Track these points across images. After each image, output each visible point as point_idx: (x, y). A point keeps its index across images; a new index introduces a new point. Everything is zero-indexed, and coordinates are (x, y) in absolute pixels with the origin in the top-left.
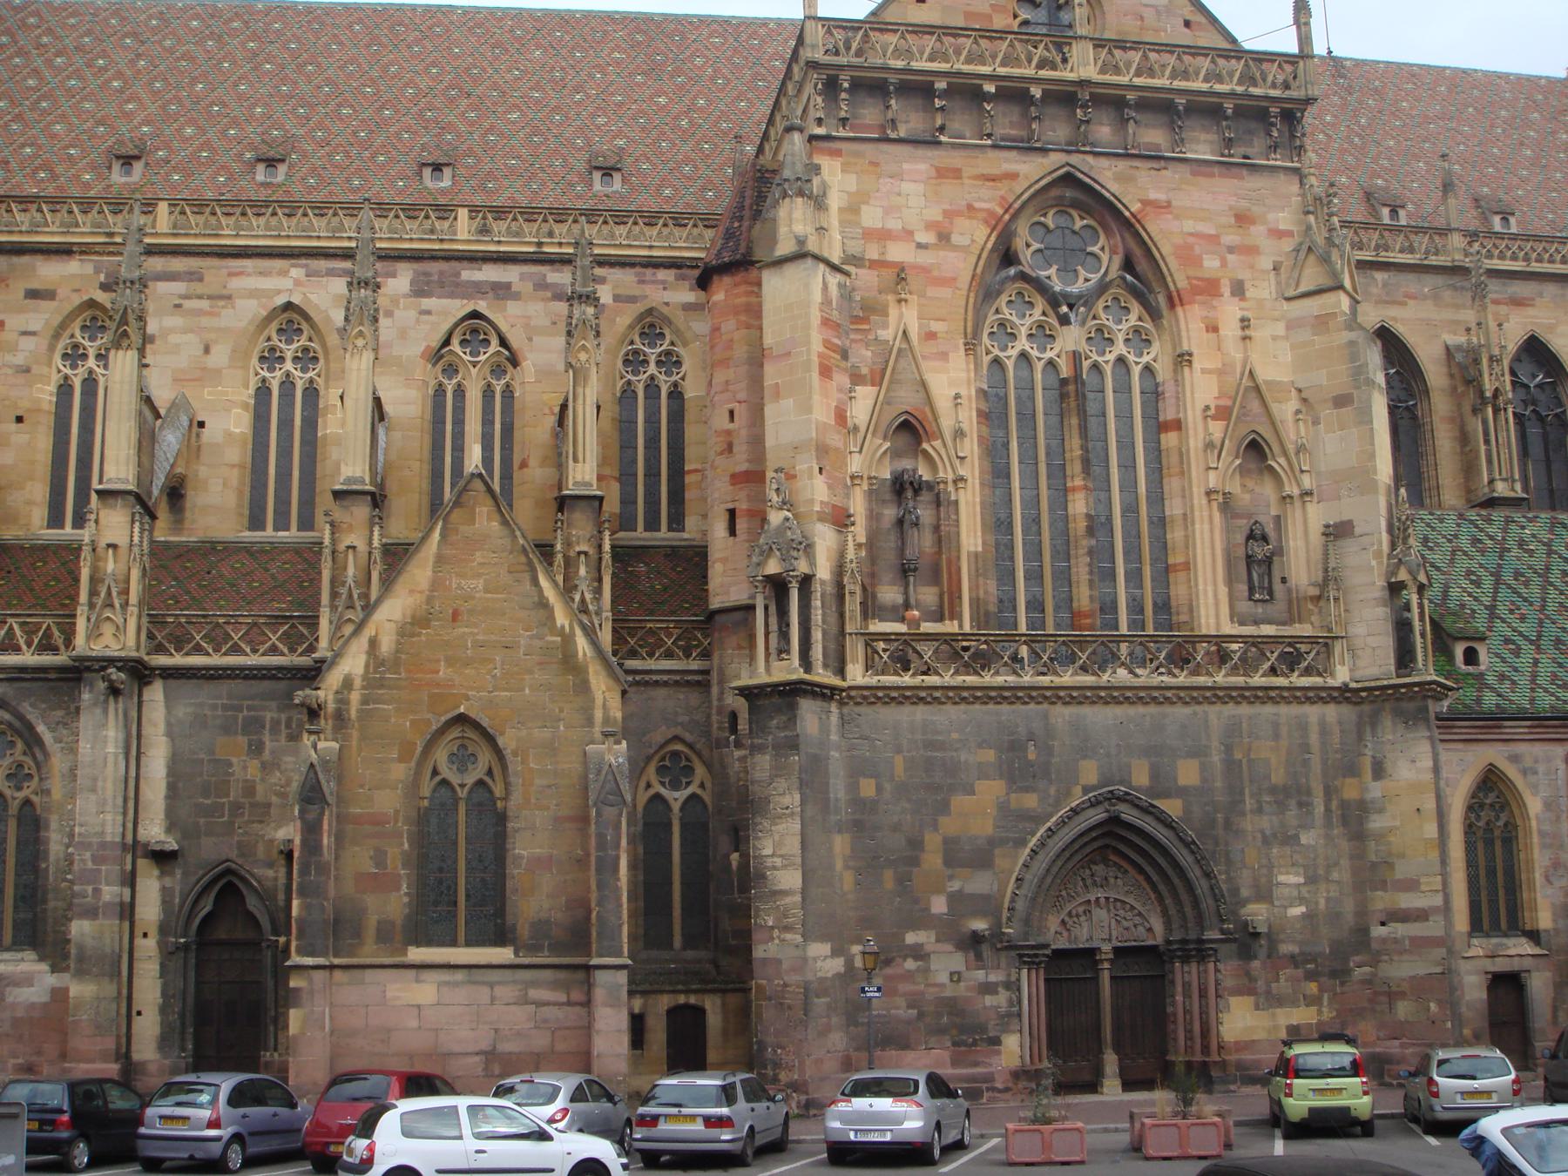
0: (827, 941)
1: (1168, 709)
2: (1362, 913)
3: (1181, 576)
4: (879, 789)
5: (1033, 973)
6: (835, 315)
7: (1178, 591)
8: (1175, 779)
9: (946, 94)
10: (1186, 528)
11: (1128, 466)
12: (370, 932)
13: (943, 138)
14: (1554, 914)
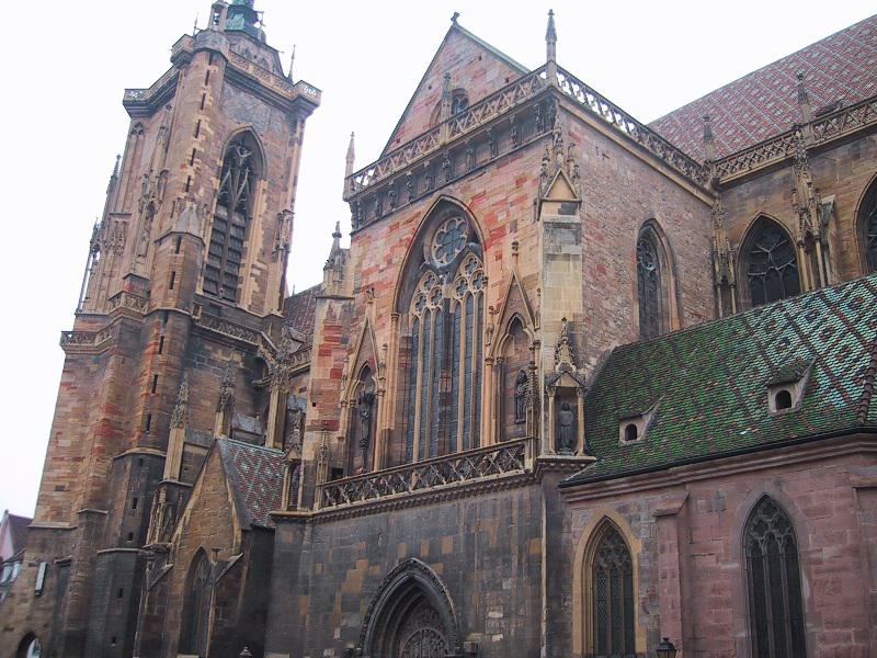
0: (286, 653)
1: (441, 506)
6: (338, 323)
8: (441, 551)
11: (467, 358)
12: (170, 647)
14: (649, 639)
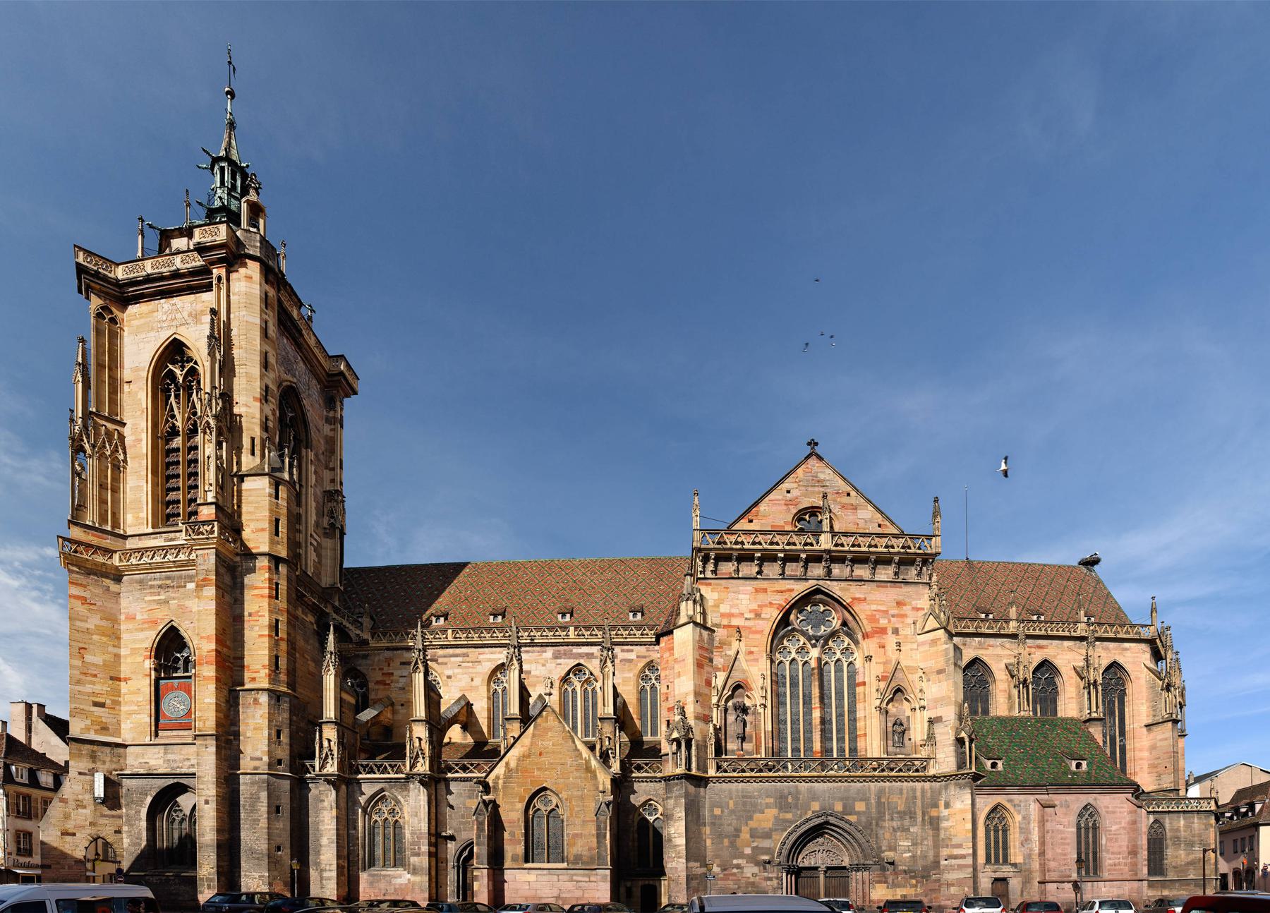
2: (937, 856)
3: (863, 739)
4: (722, 812)
5: (789, 876)
6: (706, 646)
7: (861, 744)
9: (759, 559)
10: (865, 721)
13: (759, 576)
